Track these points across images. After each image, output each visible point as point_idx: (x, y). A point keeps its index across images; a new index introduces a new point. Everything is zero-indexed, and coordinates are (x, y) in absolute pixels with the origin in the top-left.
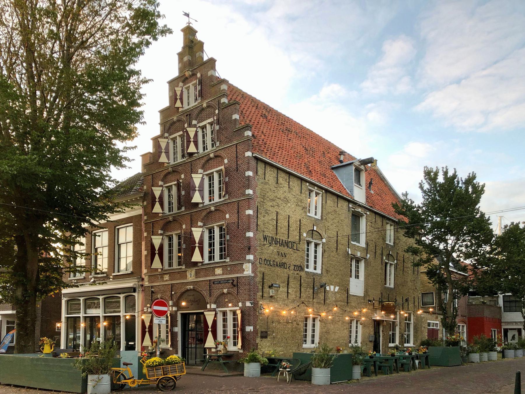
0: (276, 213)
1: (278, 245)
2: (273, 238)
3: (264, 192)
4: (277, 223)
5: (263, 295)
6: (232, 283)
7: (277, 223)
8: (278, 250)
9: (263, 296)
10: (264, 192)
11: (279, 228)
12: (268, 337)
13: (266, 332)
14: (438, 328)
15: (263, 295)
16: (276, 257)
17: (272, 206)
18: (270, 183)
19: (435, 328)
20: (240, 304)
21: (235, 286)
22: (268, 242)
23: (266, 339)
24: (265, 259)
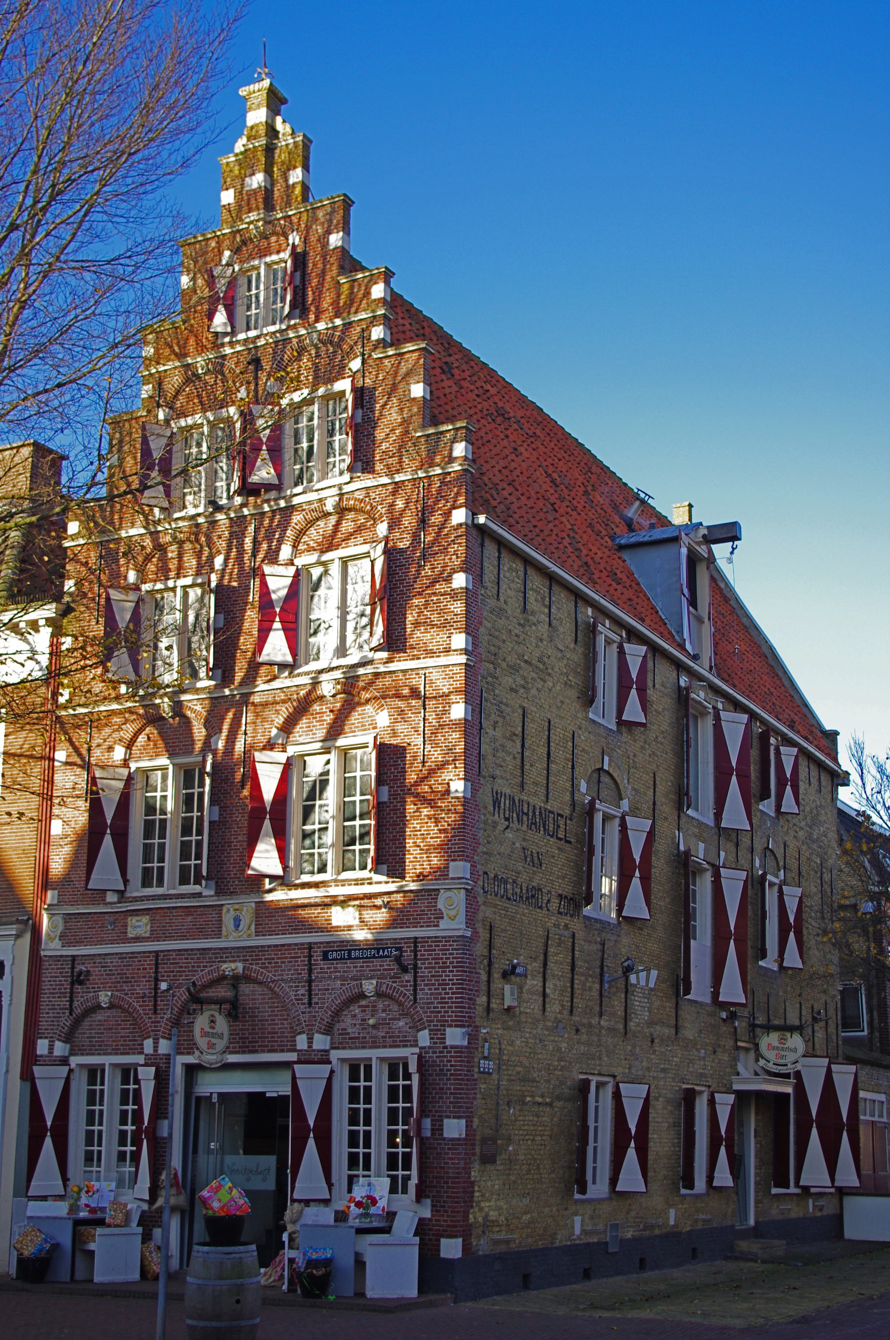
0: (520, 711)
1: (525, 827)
2: (514, 801)
3: (495, 641)
4: (523, 746)
5: (489, 1003)
6: (398, 959)
7: (523, 746)
8: (524, 844)
9: (488, 1009)
10: (495, 641)
11: (527, 767)
12: (498, 1158)
13: (494, 1140)
14: (885, 1119)
15: (489, 1003)
16: (520, 866)
17: (512, 689)
18: (509, 611)
19: (876, 1119)
20: (424, 1038)
21: (405, 970)
22: (502, 815)
23: (492, 1168)
24: (496, 876)
